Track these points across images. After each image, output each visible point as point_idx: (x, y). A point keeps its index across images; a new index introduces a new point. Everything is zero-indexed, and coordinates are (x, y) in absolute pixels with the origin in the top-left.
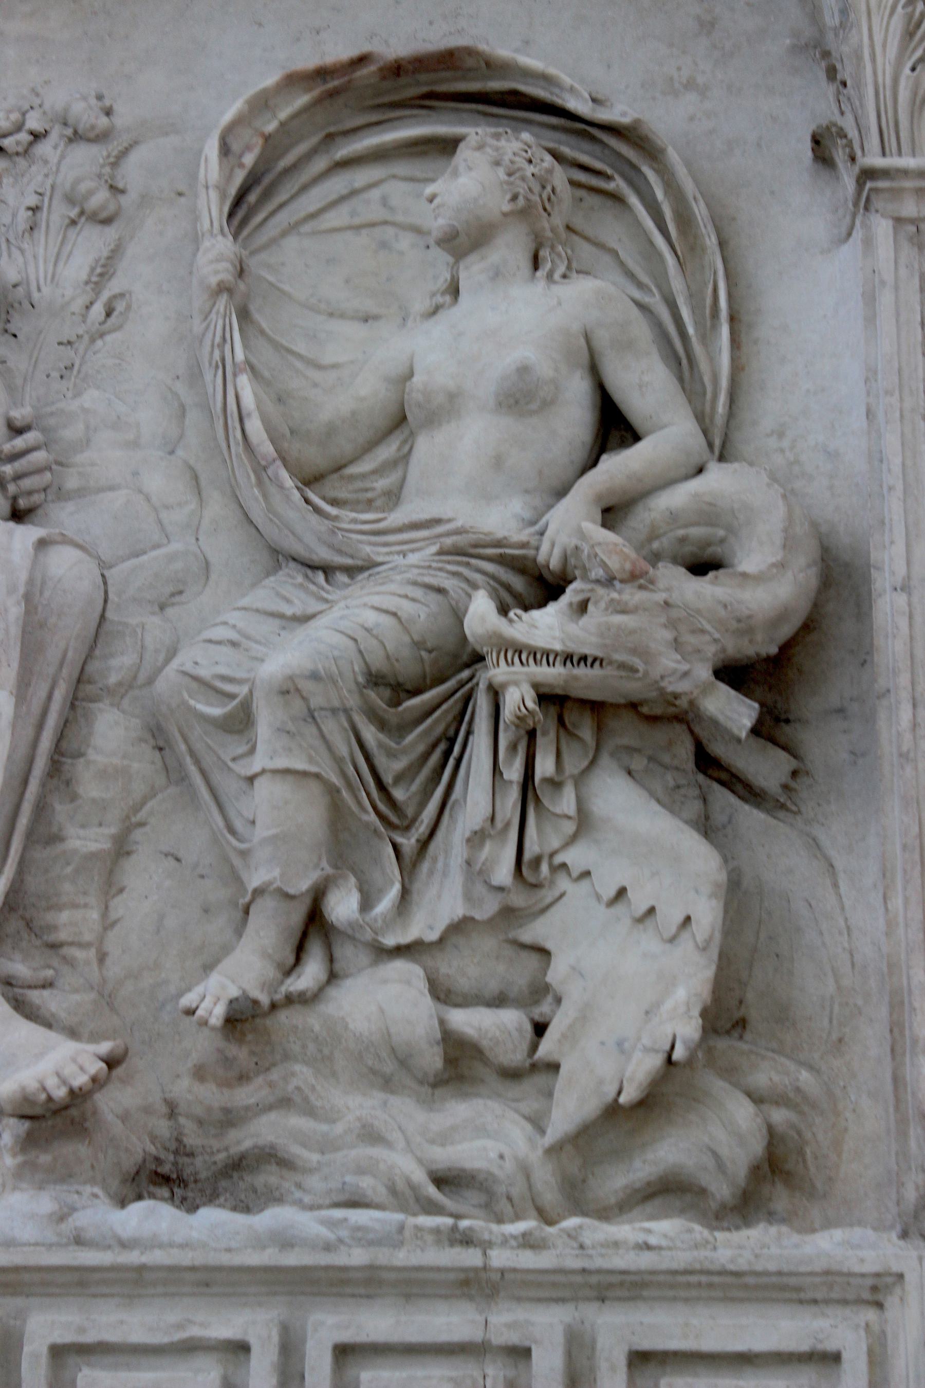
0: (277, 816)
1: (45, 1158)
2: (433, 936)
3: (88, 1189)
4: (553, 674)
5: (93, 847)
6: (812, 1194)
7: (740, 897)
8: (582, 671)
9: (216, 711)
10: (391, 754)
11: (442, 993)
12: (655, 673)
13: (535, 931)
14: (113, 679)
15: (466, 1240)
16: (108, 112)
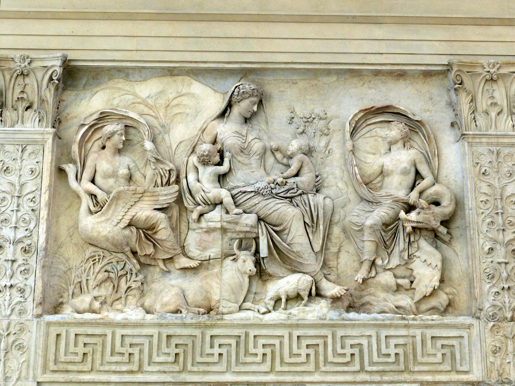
0: (369, 247)
1: (335, 305)
2: (394, 267)
3: (342, 310)
4: (414, 225)
5: (336, 251)
6: (455, 309)
7: (444, 261)
8: (419, 224)
9: (357, 229)
10: (386, 237)
11: (395, 276)
12: (431, 225)
13: (411, 266)
14: (336, 221)
15: (404, 319)
16: (326, 114)
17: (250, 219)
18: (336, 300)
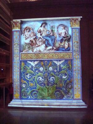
0: (59, 42)
17: (45, 40)
18: (55, 49)
